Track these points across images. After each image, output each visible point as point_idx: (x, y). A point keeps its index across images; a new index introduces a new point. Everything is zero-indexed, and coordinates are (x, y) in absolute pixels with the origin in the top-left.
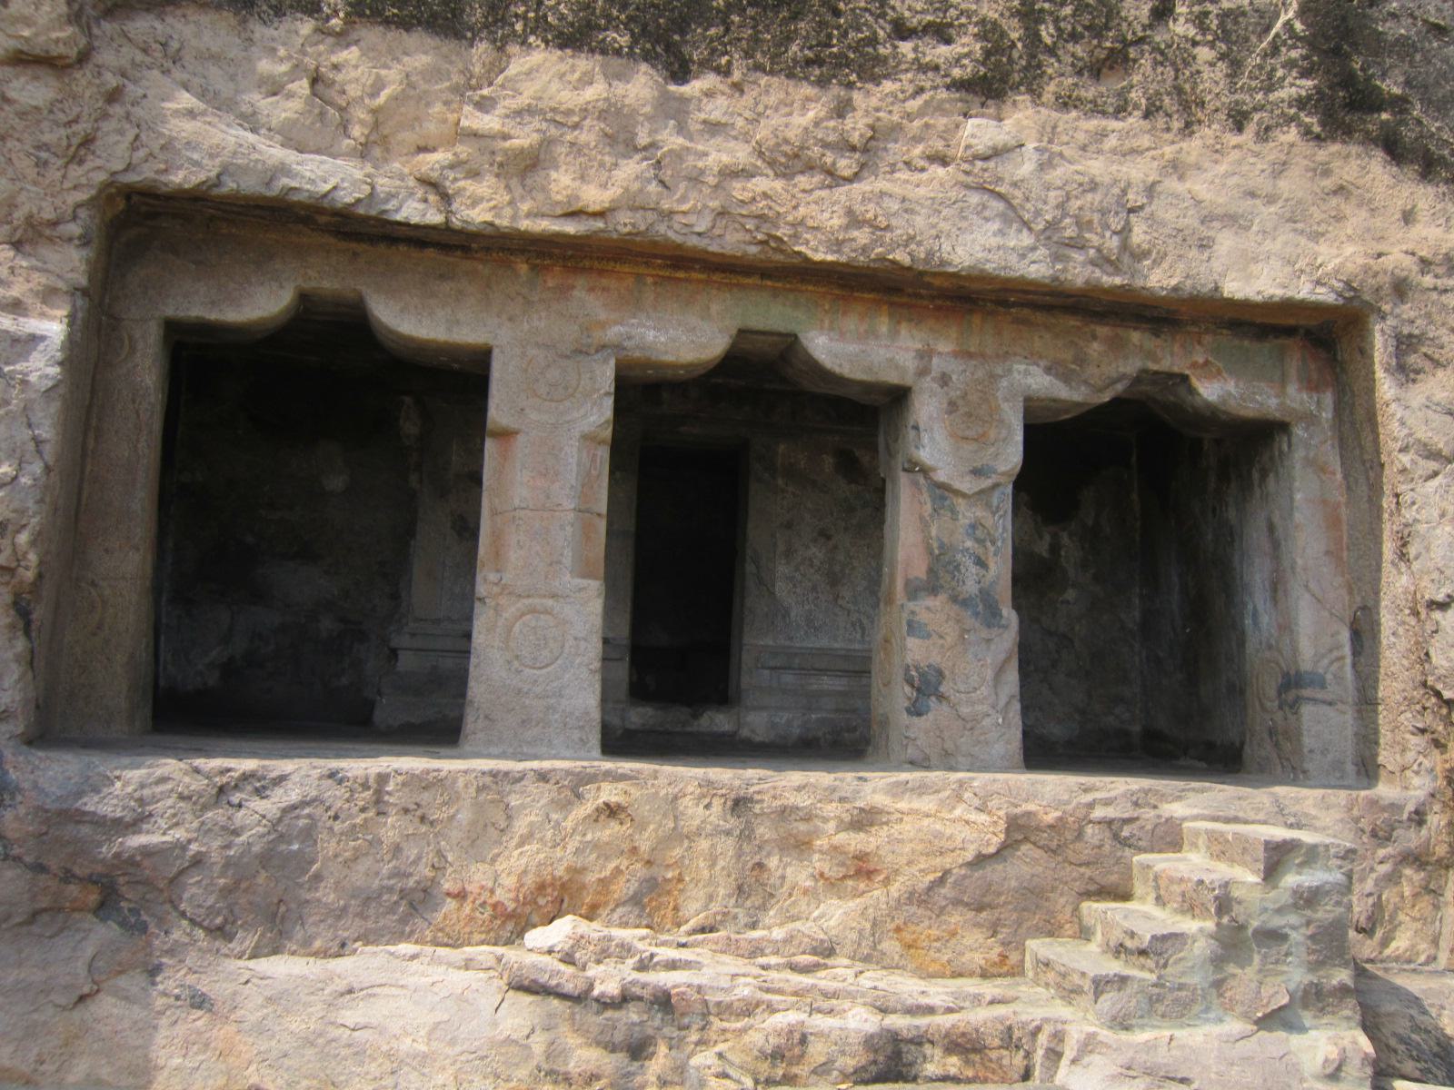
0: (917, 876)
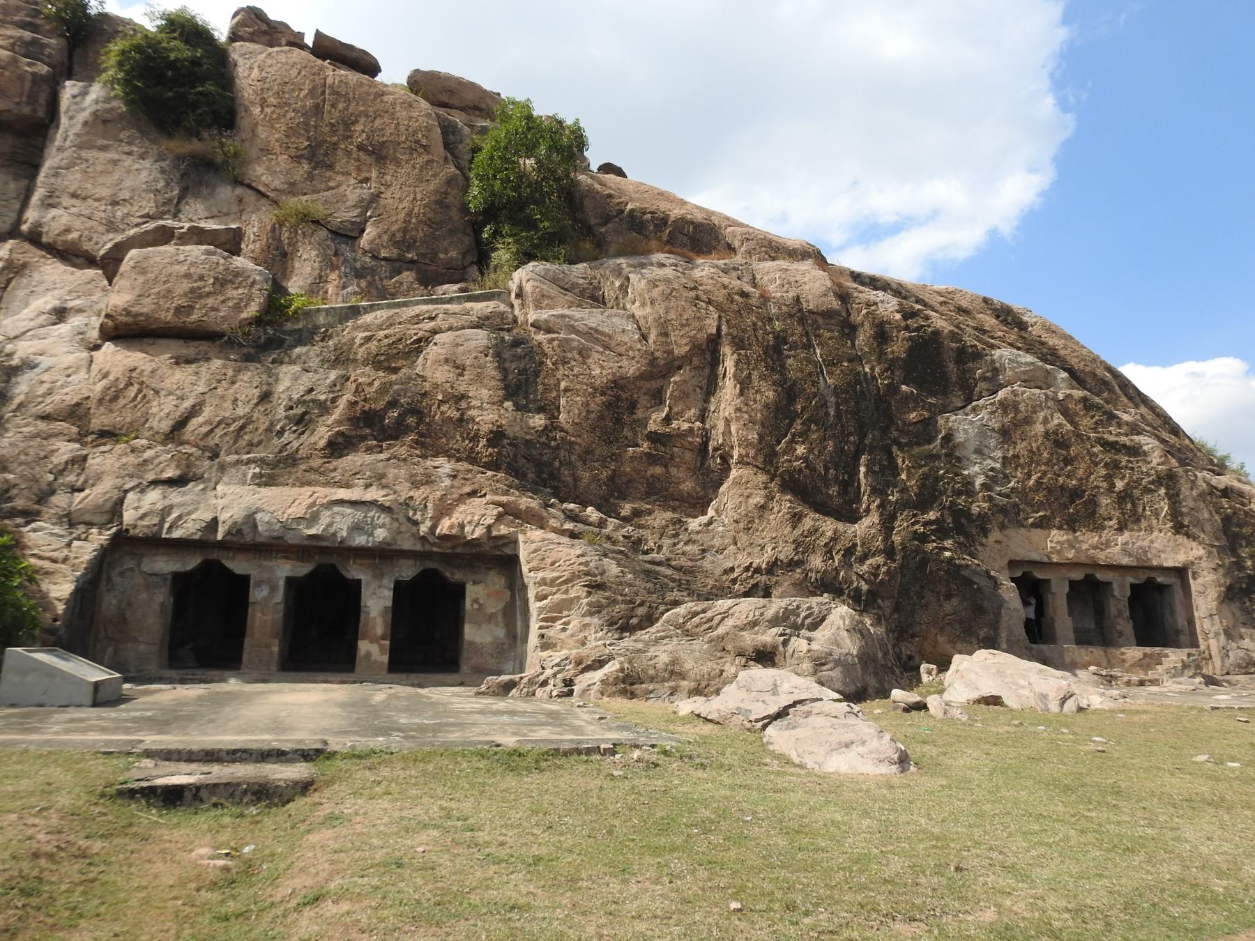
0: (1131, 662)
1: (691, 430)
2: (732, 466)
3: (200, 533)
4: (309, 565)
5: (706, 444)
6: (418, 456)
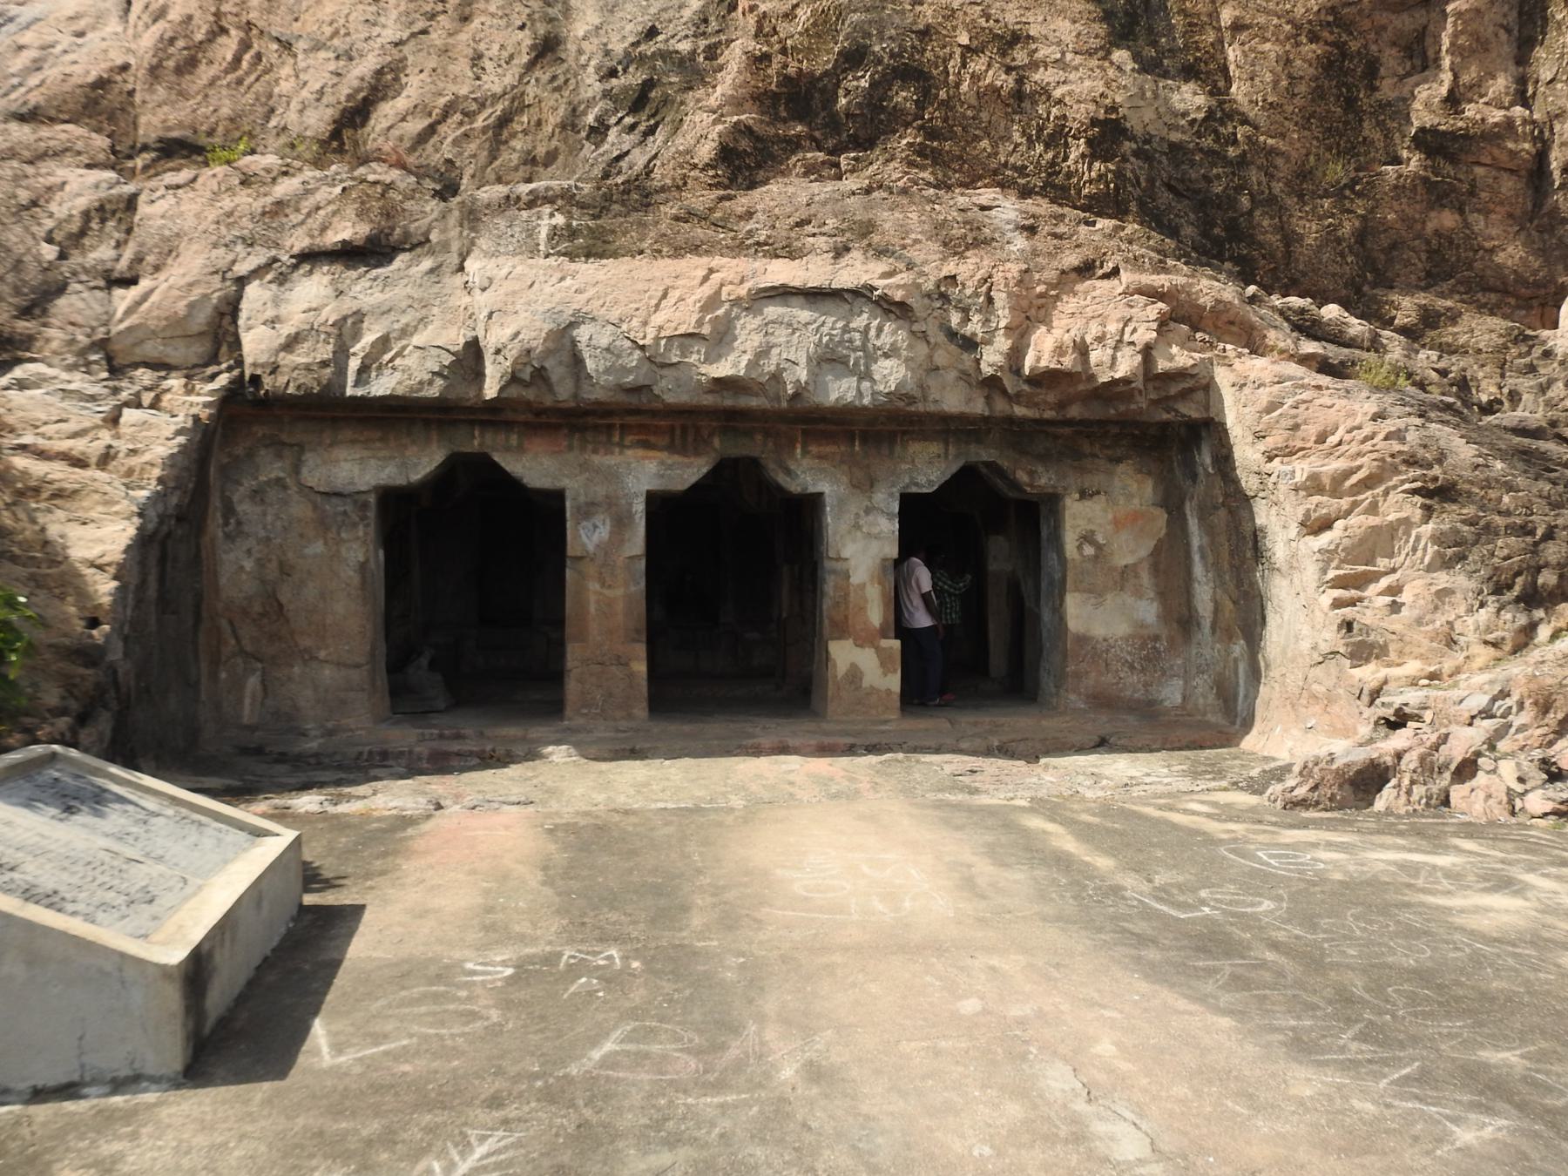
3: (439, 382)
5: (1542, 157)
6: (929, 184)
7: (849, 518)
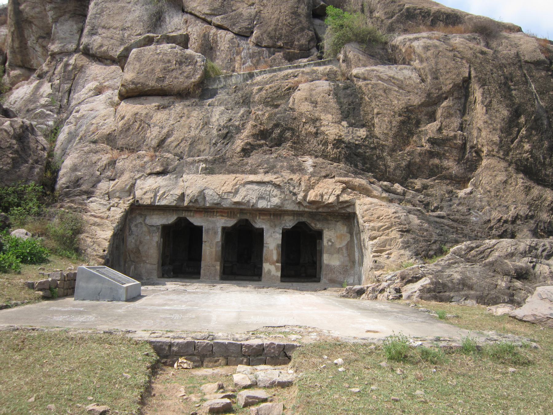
1: (455, 137)
2: (483, 158)
3: (175, 202)
4: (234, 220)
5: (465, 144)
6: (293, 155)
7: (269, 234)
